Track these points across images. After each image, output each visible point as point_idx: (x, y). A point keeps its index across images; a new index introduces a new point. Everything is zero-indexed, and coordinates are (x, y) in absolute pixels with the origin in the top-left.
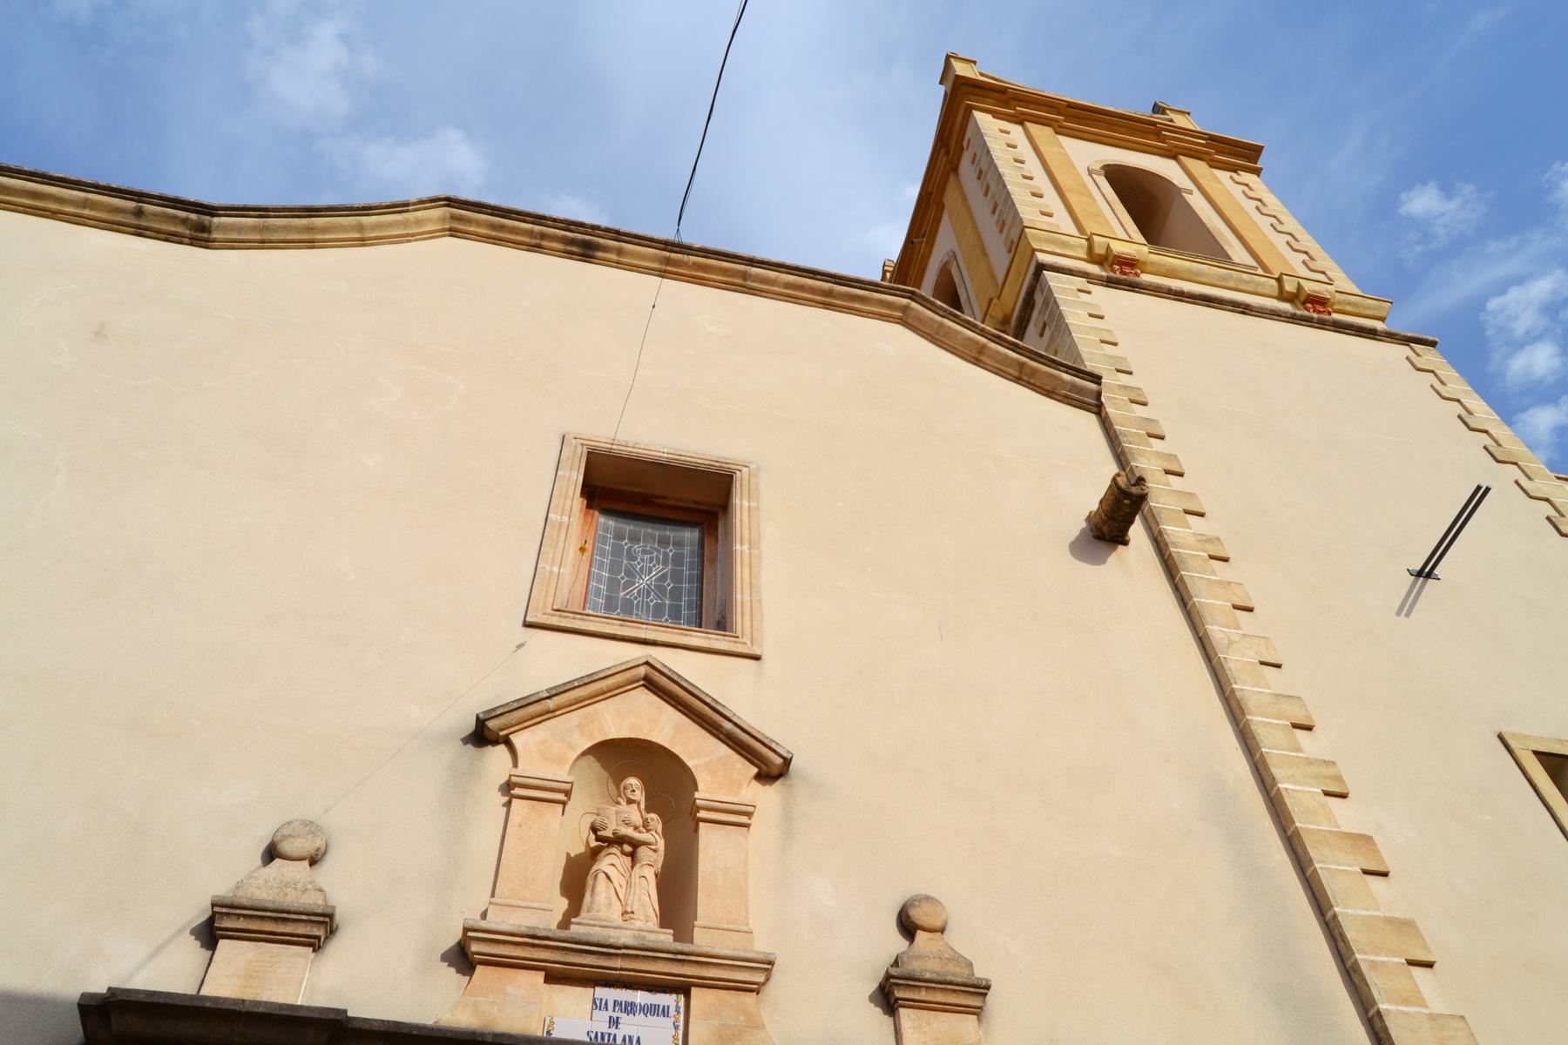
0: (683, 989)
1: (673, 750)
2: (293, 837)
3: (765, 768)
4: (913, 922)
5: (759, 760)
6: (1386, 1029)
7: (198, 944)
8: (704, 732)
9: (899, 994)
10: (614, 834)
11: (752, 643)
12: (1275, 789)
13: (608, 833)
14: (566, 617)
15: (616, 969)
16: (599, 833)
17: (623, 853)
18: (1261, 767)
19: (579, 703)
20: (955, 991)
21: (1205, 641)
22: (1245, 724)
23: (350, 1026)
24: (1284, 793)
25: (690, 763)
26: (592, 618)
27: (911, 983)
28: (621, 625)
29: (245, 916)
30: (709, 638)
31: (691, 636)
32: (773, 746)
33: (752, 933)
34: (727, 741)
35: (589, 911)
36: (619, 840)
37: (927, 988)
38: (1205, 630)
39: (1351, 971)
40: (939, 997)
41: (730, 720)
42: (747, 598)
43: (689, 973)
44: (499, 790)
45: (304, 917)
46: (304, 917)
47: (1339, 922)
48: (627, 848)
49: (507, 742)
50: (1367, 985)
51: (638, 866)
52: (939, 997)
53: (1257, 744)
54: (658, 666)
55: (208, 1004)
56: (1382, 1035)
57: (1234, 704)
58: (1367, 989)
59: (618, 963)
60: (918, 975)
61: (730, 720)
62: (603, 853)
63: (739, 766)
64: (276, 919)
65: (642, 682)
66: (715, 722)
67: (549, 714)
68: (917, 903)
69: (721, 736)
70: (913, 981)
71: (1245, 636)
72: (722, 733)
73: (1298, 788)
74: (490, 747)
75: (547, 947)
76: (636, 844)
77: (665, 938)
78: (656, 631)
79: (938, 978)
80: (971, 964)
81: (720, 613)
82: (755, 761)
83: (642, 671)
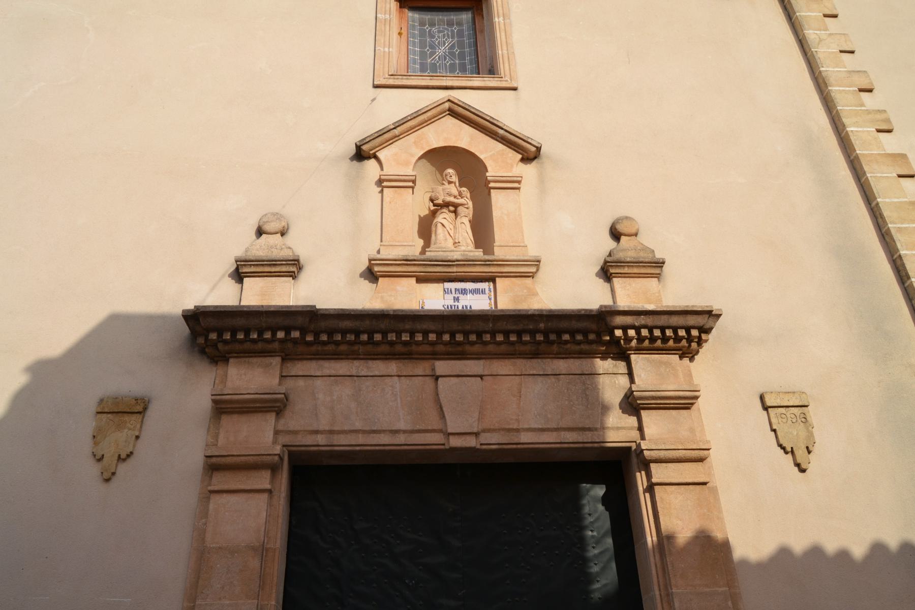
0: (492, 279)
1: (471, 150)
2: (269, 222)
3: (526, 154)
4: (619, 232)
5: (522, 150)
6: (903, 265)
7: (234, 281)
8: (487, 138)
9: (612, 271)
10: (443, 201)
11: (511, 80)
12: (845, 131)
13: (440, 201)
14: (398, 79)
15: (453, 273)
16: (435, 202)
17: (450, 211)
18: (836, 119)
19: (413, 130)
20: (644, 266)
21: (803, 42)
22: (827, 93)
23: (319, 313)
24: (850, 134)
25: (482, 157)
26: (413, 77)
27: (619, 264)
28: (431, 79)
29: (254, 265)
30: (484, 80)
31: (473, 80)
32: (529, 140)
33: (526, 246)
34: (502, 141)
35: (435, 244)
36: (446, 205)
37: (628, 266)
38: (804, 34)
39: (885, 234)
40: (635, 270)
41: (502, 129)
42: (505, 52)
43: (494, 271)
44: (375, 185)
45: (284, 263)
46: (284, 263)
47: (879, 207)
48: (452, 208)
49: (375, 157)
50: (894, 241)
51: (459, 217)
52: (635, 270)
53: (835, 105)
54: (456, 101)
55: (245, 309)
56: (901, 268)
57: (821, 81)
58: (894, 243)
59: (455, 269)
60: (623, 260)
61: (502, 129)
62: (439, 212)
63: (510, 155)
64: (270, 265)
65: (448, 112)
66: (494, 131)
67: (396, 138)
68: (620, 221)
69: (498, 139)
70: (620, 263)
71: (830, 34)
72: (498, 136)
73: (860, 129)
74: (366, 161)
75: (415, 265)
76: (456, 206)
77: (479, 254)
78: (452, 80)
79: (634, 260)
80: (653, 251)
81: (490, 64)
82: (520, 151)
83: (447, 105)
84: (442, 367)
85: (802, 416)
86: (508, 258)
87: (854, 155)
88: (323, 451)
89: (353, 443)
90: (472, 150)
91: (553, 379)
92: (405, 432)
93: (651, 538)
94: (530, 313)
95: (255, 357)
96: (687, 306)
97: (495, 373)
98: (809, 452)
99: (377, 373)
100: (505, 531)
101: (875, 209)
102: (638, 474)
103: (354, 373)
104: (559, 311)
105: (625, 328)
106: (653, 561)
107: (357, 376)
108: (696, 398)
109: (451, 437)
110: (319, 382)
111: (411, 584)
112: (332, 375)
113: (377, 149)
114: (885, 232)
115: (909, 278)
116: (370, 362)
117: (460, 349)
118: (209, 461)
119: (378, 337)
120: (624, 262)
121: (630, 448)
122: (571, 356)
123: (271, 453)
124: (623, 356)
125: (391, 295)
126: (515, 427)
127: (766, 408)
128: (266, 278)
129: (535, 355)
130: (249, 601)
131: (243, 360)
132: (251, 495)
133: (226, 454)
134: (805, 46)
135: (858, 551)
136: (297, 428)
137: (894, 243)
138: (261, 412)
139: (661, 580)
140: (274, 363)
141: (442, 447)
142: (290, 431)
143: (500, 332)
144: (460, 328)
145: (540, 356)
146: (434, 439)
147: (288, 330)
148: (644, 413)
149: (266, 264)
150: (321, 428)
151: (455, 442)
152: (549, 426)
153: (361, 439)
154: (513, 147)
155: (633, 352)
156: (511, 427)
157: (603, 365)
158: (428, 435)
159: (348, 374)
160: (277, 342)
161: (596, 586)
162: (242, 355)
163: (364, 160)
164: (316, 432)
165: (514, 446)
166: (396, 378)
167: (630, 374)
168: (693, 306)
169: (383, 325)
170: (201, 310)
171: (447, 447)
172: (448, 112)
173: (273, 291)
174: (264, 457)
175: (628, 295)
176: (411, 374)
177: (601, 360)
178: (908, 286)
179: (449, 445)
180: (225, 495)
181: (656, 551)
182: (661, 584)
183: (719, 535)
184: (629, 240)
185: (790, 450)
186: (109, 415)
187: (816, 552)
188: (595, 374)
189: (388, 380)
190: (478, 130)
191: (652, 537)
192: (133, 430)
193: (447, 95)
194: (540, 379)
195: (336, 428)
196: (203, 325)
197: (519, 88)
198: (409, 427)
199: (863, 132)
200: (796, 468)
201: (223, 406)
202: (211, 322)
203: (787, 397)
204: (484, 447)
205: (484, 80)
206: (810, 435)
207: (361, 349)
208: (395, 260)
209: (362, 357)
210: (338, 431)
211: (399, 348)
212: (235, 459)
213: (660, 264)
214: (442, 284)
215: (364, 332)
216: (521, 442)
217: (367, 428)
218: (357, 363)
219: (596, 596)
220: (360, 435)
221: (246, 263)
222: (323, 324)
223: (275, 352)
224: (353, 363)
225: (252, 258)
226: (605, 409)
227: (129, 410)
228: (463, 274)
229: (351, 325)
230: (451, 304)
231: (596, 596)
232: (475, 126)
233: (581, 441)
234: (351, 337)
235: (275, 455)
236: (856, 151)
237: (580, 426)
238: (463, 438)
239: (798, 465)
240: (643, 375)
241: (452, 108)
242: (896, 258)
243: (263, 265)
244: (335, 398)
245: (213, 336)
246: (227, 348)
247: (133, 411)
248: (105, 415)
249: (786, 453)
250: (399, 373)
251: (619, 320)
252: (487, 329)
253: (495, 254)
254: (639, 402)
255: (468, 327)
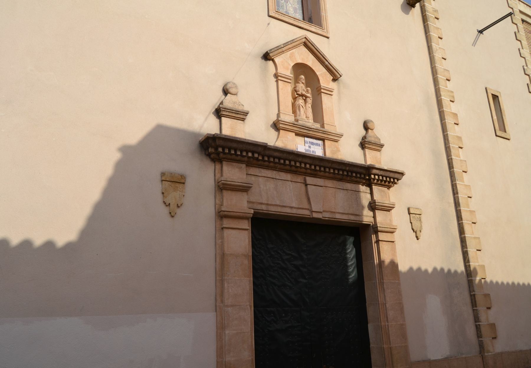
0: (323, 140)
1: (313, 68)
2: (232, 88)
3: (335, 77)
4: (368, 127)
5: (334, 75)
6: (452, 162)
7: (215, 117)
8: (319, 63)
9: (366, 146)
10: (301, 93)
11: (327, 32)
12: (440, 98)
13: (300, 93)
14: (280, 15)
15: (310, 134)
16: (298, 93)
17: (303, 99)
18: (438, 91)
19: (290, 49)
20: (377, 146)
21: (430, 48)
22: (436, 77)
23: (267, 147)
24: (442, 99)
25: (318, 73)
26: (286, 16)
27: (369, 143)
28: (294, 20)
29: (228, 111)
30: (316, 29)
31: (312, 27)
32: (338, 71)
33: (336, 126)
34: (326, 67)
35: (299, 116)
36: (302, 95)
37: (372, 145)
38: (431, 44)
39: (447, 147)
40: (374, 147)
41: (327, 61)
42: (324, 14)
43: (325, 137)
44: (274, 76)
45: (242, 113)
46: (242, 113)
47: (448, 136)
48: (304, 98)
49: (273, 60)
50: (451, 152)
51: (307, 104)
52: (374, 147)
53: (438, 84)
54: (309, 39)
55: (238, 140)
56: (451, 163)
57: (434, 70)
58: (450, 152)
59: (311, 132)
60: (371, 142)
61: (327, 61)
62: (298, 98)
63: (328, 76)
64: (235, 113)
65: (303, 44)
66: (323, 61)
67: (283, 52)
68: (369, 122)
69: (324, 66)
70: (370, 143)
71: (440, 48)
72: (324, 65)
73: (445, 99)
74: (268, 61)
75: (296, 127)
76: (306, 97)
77: (317, 126)
78: (303, 24)
79: (375, 143)
80: (380, 139)
81: (310, 15)
82: (333, 75)
83: (304, 40)
84: (309, 180)
85: (420, 218)
86: (332, 132)
87: (442, 109)
88: (264, 213)
89: (277, 211)
90: (314, 68)
91: (346, 192)
92: (295, 208)
93: (376, 261)
94: (345, 162)
95: (234, 162)
96: (397, 170)
97: (326, 186)
98: (420, 232)
99: (283, 179)
100: (321, 253)
101: (446, 136)
102: (373, 235)
103: (274, 177)
104: (355, 163)
105: (375, 175)
106: (377, 269)
107: (275, 179)
108: (394, 208)
109: (313, 213)
110: (261, 179)
111: (289, 272)
112: (265, 176)
113: (275, 56)
114: (447, 147)
115: (453, 168)
116: (280, 173)
117: (316, 173)
118: (224, 213)
119: (287, 162)
120: (371, 143)
121: (370, 225)
122: (352, 182)
123: (250, 212)
124: (369, 185)
125: (286, 140)
126: (334, 211)
127: (409, 214)
128: (232, 119)
129: (341, 180)
130: (246, 278)
131: (229, 163)
132: (241, 231)
133: (231, 211)
134: (430, 50)
135: (430, 270)
136: (254, 201)
137: (450, 152)
138: (241, 191)
139: (379, 277)
140: (243, 167)
141: (309, 217)
142: (251, 202)
143: (332, 168)
144: (319, 164)
145: (342, 181)
146: (306, 213)
147: (253, 153)
148: (376, 211)
149: (234, 112)
150: (264, 202)
151: (315, 215)
152: (345, 212)
153: (279, 209)
154: (330, 72)
155: (374, 185)
156: (332, 211)
157: (363, 188)
158: (304, 210)
159: (272, 177)
160: (246, 157)
161: (351, 277)
162: (229, 160)
163: (267, 61)
164: (261, 204)
165: (334, 219)
166: (290, 182)
167: (372, 193)
168: (398, 170)
169: (291, 157)
170: (219, 136)
171: (311, 217)
172: (303, 44)
173: (236, 127)
174: (247, 214)
175: (370, 158)
176: (296, 181)
177: (362, 186)
178: (452, 171)
179: (312, 216)
180: (230, 230)
181: (378, 266)
182: (379, 278)
183: (396, 261)
184: (372, 132)
185: (415, 231)
186: (169, 182)
187: (419, 269)
188: (359, 191)
189: (287, 182)
190: (316, 58)
191: (376, 260)
192: (182, 192)
193: (304, 34)
194: (342, 191)
195: (270, 203)
196: (217, 143)
197: (330, 38)
198: (297, 206)
199: (446, 100)
200: (416, 238)
201: (226, 186)
202: (221, 143)
203: (416, 210)
204: (324, 218)
205: (316, 29)
206: (421, 226)
207: (279, 166)
208: (289, 123)
209: (277, 170)
210: (270, 204)
211: (293, 168)
212: (235, 213)
213: (382, 146)
214: (303, 138)
215: (282, 159)
216: (336, 218)
217: (281, 204)
218: (275, 172)
219: (351, 280)
220: (279, 207)
221: (225, 110)
222: (267, 152)
223: (244, 162)
224: (273, 172)
225: (229, 108)
226: (363, 208)
227: (178, 181)
228: (314, 135)
229: (278, 155)
230: (307, 149)
231: (351, 280)
232: (315, 56)
233: (356, 220)
234: (277, 160)
235: (251, 214)
236: (443, 108)
237: (355, 213)
238: (318, 214)
239: (417, 237)
240: (376, 195)
241: (306, 42)
242: (450, 159)
243: (232, 112)
244: (268, 188)
245: (220, 150)
246: (224, 156)
247: (181, 182)
248: (167, 182)
249: (414, 232)
250: (291, 180)
251: (374, 171)
252: (328, 166)
253: (325, 128)
254: (376, 207)
255: (322, 164)
